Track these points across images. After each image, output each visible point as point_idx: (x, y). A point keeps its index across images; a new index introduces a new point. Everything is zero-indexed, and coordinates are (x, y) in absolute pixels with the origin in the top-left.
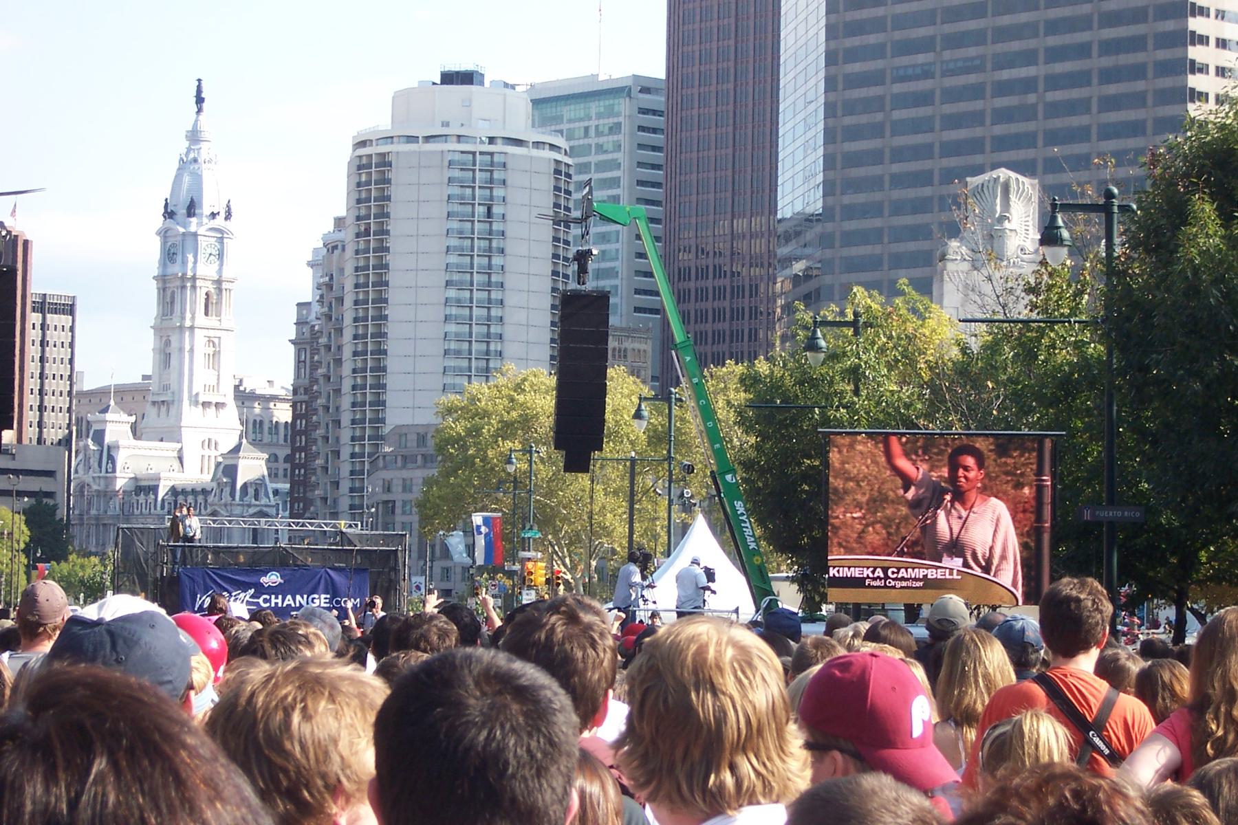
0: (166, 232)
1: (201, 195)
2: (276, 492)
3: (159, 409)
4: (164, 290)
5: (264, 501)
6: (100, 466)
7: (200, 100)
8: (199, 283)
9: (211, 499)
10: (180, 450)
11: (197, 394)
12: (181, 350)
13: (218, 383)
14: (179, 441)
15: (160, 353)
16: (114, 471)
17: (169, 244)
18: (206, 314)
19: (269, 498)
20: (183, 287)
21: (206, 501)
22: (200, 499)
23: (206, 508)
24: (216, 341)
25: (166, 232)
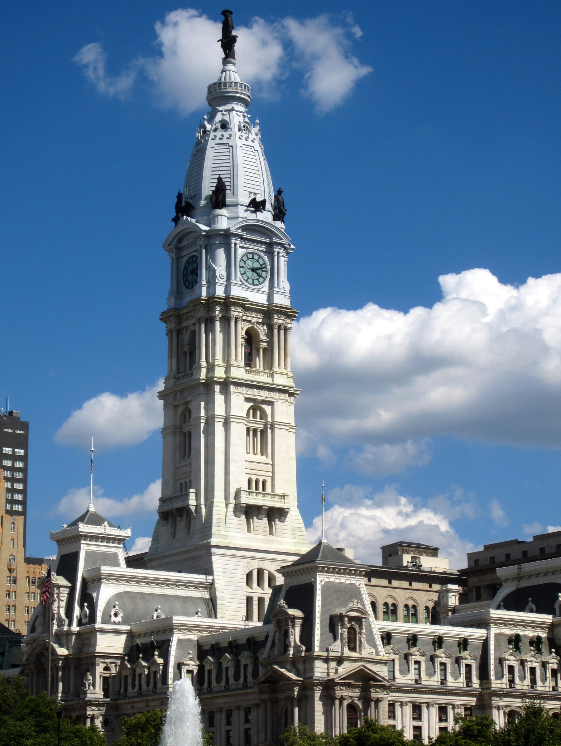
0: (180, 241)
1: (233, 177)
2: (387, 638)
3: (174, 526)
4: (179, 332)
5: (366, 651)
8: (235, 312)
9: (264, 654)
10: (211, 587)
11: (238, 493)
12: (210, 421)
14: (209, 571)
15: (175, 433)
16: (92, 618)
17: (185, 259)
18: (249, 361)
19: (375, 646)
20: (210, 322)
21: (256, 660)
22: (245, 658)
23: (255, 674)
24: (268, 409)
25: (180, 241)
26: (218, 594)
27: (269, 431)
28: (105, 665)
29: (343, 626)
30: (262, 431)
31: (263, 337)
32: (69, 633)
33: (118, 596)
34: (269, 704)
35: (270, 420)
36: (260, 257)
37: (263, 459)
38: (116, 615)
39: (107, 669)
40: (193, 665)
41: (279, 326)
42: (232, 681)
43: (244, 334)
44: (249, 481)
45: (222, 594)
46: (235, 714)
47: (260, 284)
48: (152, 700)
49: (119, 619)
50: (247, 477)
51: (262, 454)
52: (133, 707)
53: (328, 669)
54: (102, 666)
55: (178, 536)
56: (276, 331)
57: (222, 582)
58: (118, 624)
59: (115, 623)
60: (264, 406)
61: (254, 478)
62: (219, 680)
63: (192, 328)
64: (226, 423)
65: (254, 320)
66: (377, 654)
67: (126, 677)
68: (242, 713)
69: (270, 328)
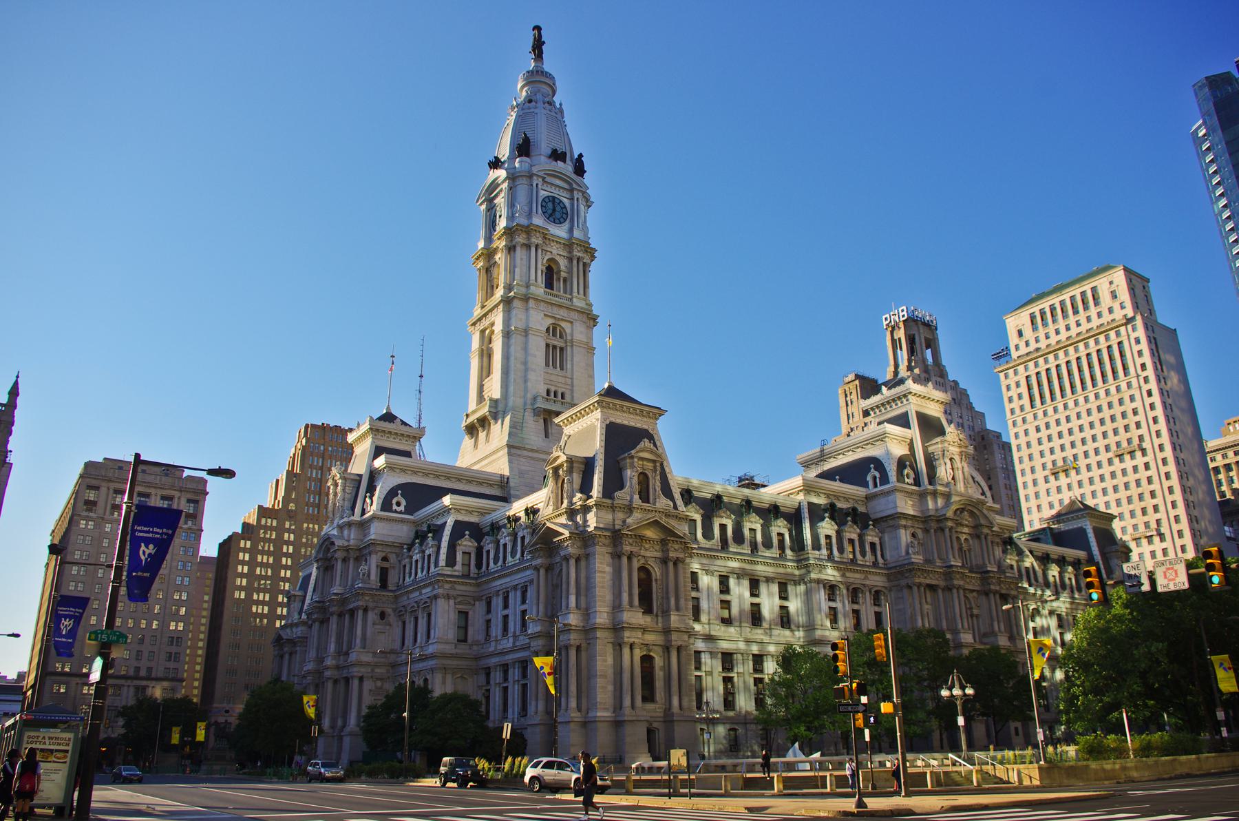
6: (353, 508)
7: (538, 48)
13: (572, 391)
18: (549, 285)
26: (512, 492)
27: (569, 348)
28: (384, 554)
29: (633, 466)
30: (561, 349)
31: (563, 268)
32: (350, 524)
33: (403, 487)
34: (542, 572)
35: (569, 338)
36: (561, 201)
37: (561, 373)
38: (398, 504)
39: (385, 559)
40: (470, 546)
41: (578, 259)
42: (509, 558)
43: (545, 262)
44: (548, 392)
45: (518, 493)
46: (511, 595)
47: (561, 223)
48: (425, 587)
49: (402, 508)
50: (546, 387)
51: (562, 369)
52: (408, 598)
53: (614, 520)
54: (381, 555)
55: (480, 446)
56: (575, 262)
57: (515, 481)
58: (401, 512)
59: (396, 512)
60: (563, 324)
61: (553, 389)
62: (496, 561)
64: (526, 332)
65: (554, 252)
66: (675, 507)
67: (405, 566)
68: (519, 594)
69: (570, 260)
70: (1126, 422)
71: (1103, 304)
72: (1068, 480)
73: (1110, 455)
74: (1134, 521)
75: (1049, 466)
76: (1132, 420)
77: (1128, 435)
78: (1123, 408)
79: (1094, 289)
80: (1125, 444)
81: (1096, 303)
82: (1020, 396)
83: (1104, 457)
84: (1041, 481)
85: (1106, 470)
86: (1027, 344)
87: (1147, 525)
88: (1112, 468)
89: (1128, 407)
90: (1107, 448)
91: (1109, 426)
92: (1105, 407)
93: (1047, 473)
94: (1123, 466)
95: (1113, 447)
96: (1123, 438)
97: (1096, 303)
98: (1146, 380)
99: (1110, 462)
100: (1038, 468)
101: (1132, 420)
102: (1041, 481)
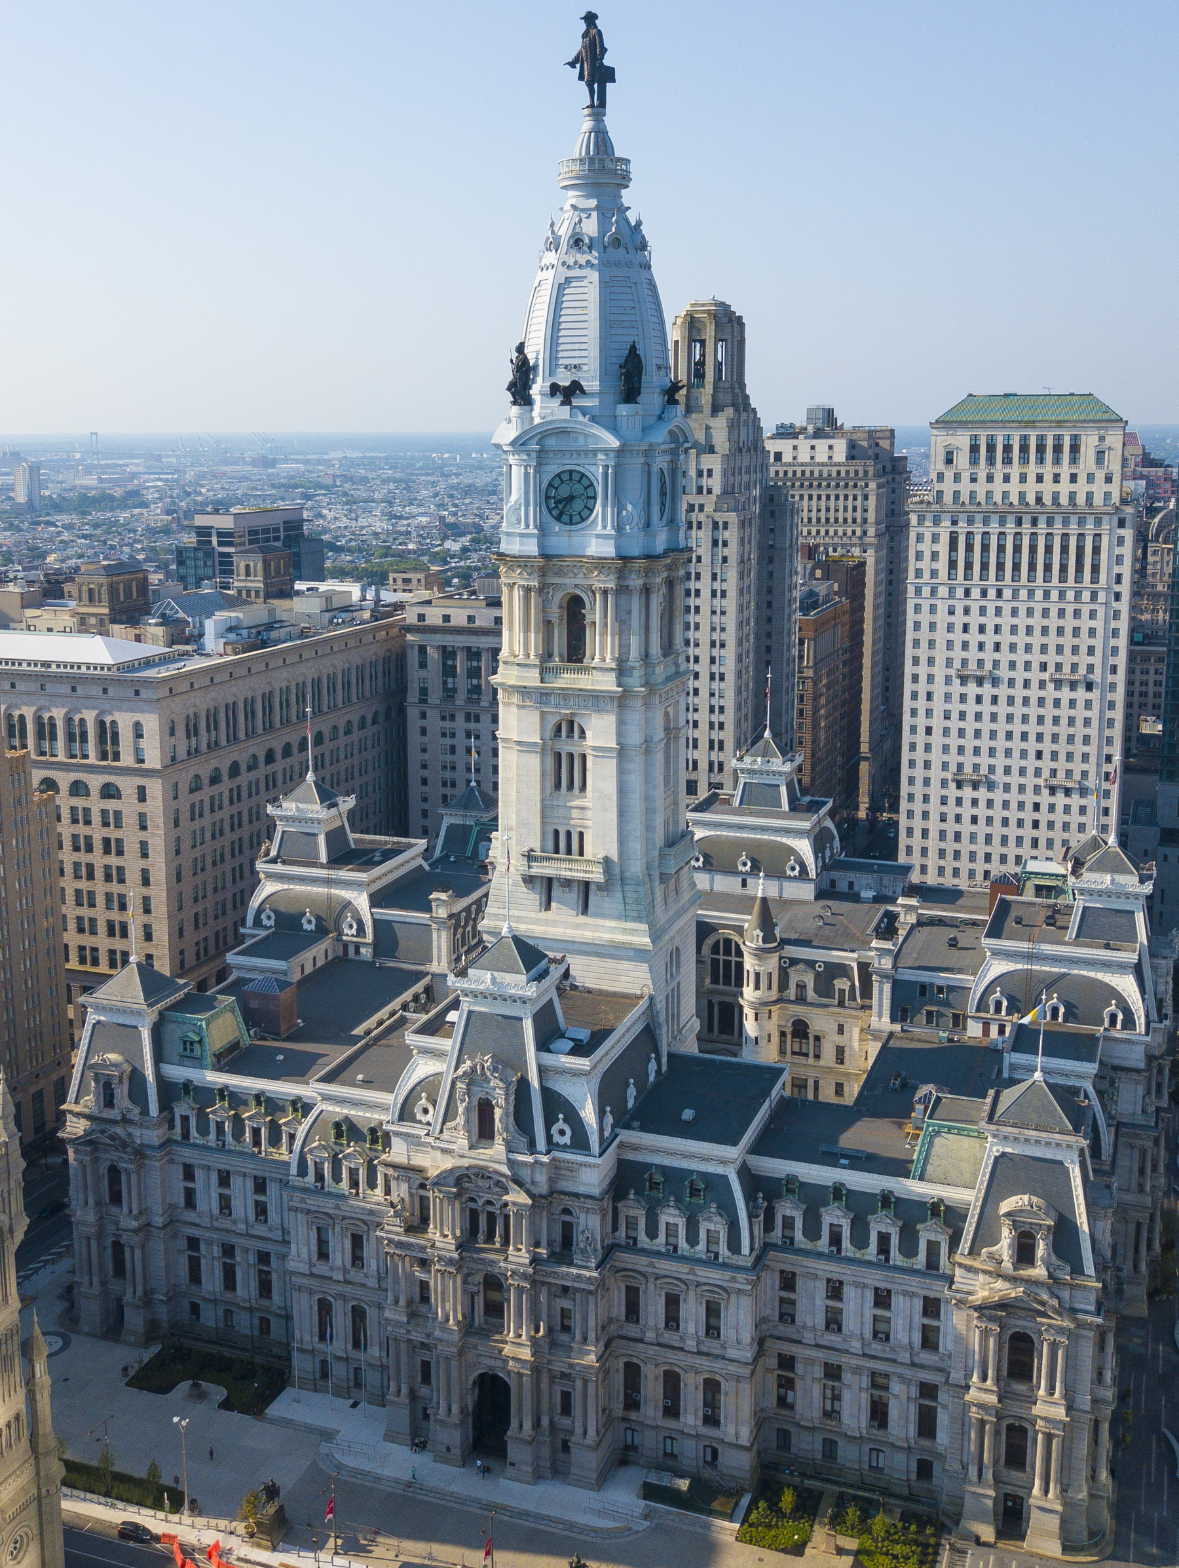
63: (571, 590)
70: (1076, 641)
71: (1082, 466)
72: (979, 691)
73: (1046, 676)
74: (1054, 765)
75: (957, 664)
76: (1084, 641)
77: (1075, 659)
78: (1077, 623)
79: (1075, 438)
80: (1067, 669)
81: (1074, 461)
82: (935, 556)
83: (1035, 675)
84: (939, 679)
85: (1034, 693)
86: (957, 478)
87: (1069, 773)
88: (1042, 694)
89: (1085, 624)
90: (1044, 667)
91: (1052, 640)
92: (1054, 613)
93: (952, 672)
94: (1058, 695)
95: (1051, 668)
96: (1067, 659)
97: (1074, 461)
98: (1118, 597)
99: (1042, 685)
100: (940, 661)
101: (1084, 641)
102: (939, 679)
